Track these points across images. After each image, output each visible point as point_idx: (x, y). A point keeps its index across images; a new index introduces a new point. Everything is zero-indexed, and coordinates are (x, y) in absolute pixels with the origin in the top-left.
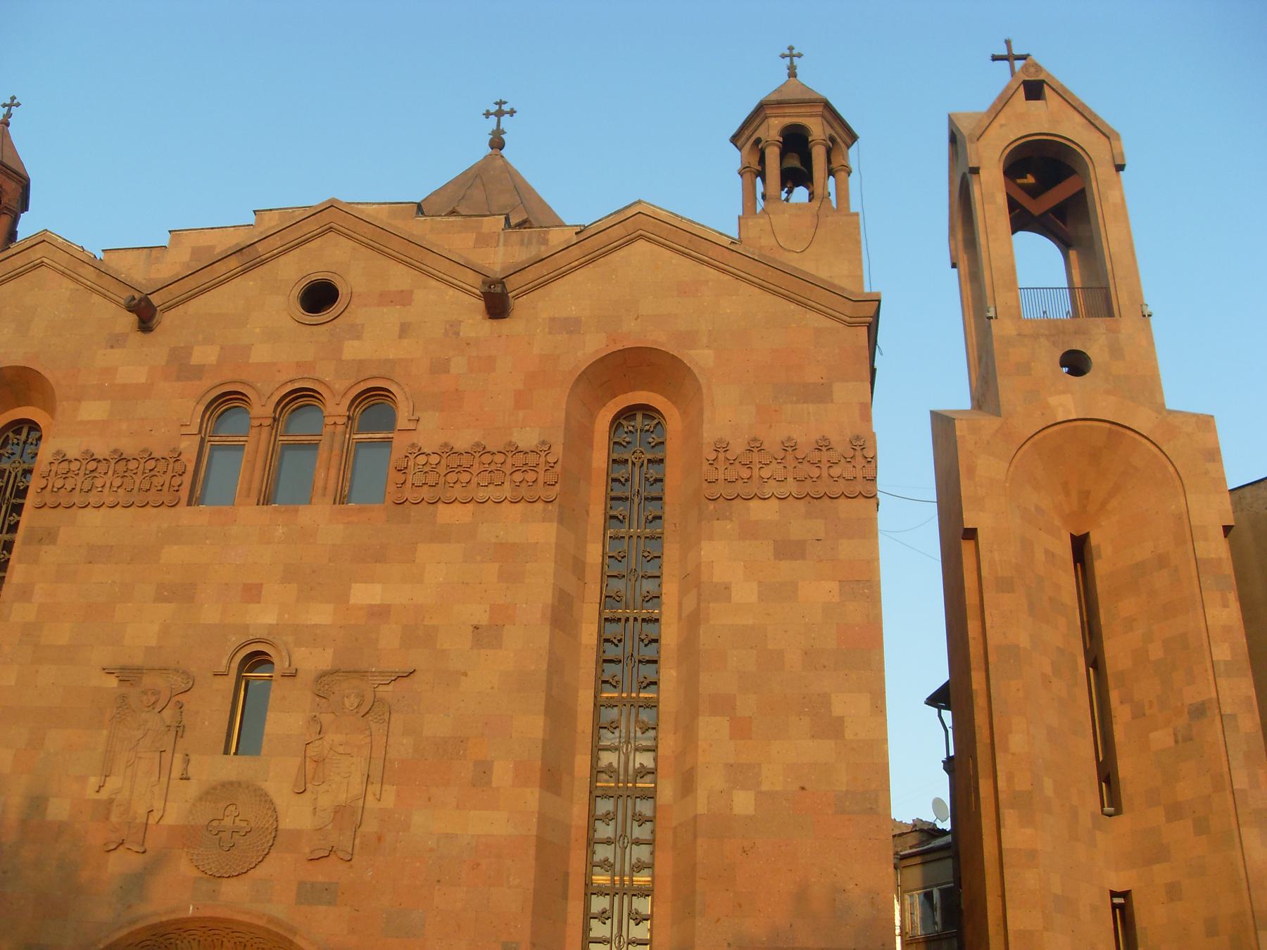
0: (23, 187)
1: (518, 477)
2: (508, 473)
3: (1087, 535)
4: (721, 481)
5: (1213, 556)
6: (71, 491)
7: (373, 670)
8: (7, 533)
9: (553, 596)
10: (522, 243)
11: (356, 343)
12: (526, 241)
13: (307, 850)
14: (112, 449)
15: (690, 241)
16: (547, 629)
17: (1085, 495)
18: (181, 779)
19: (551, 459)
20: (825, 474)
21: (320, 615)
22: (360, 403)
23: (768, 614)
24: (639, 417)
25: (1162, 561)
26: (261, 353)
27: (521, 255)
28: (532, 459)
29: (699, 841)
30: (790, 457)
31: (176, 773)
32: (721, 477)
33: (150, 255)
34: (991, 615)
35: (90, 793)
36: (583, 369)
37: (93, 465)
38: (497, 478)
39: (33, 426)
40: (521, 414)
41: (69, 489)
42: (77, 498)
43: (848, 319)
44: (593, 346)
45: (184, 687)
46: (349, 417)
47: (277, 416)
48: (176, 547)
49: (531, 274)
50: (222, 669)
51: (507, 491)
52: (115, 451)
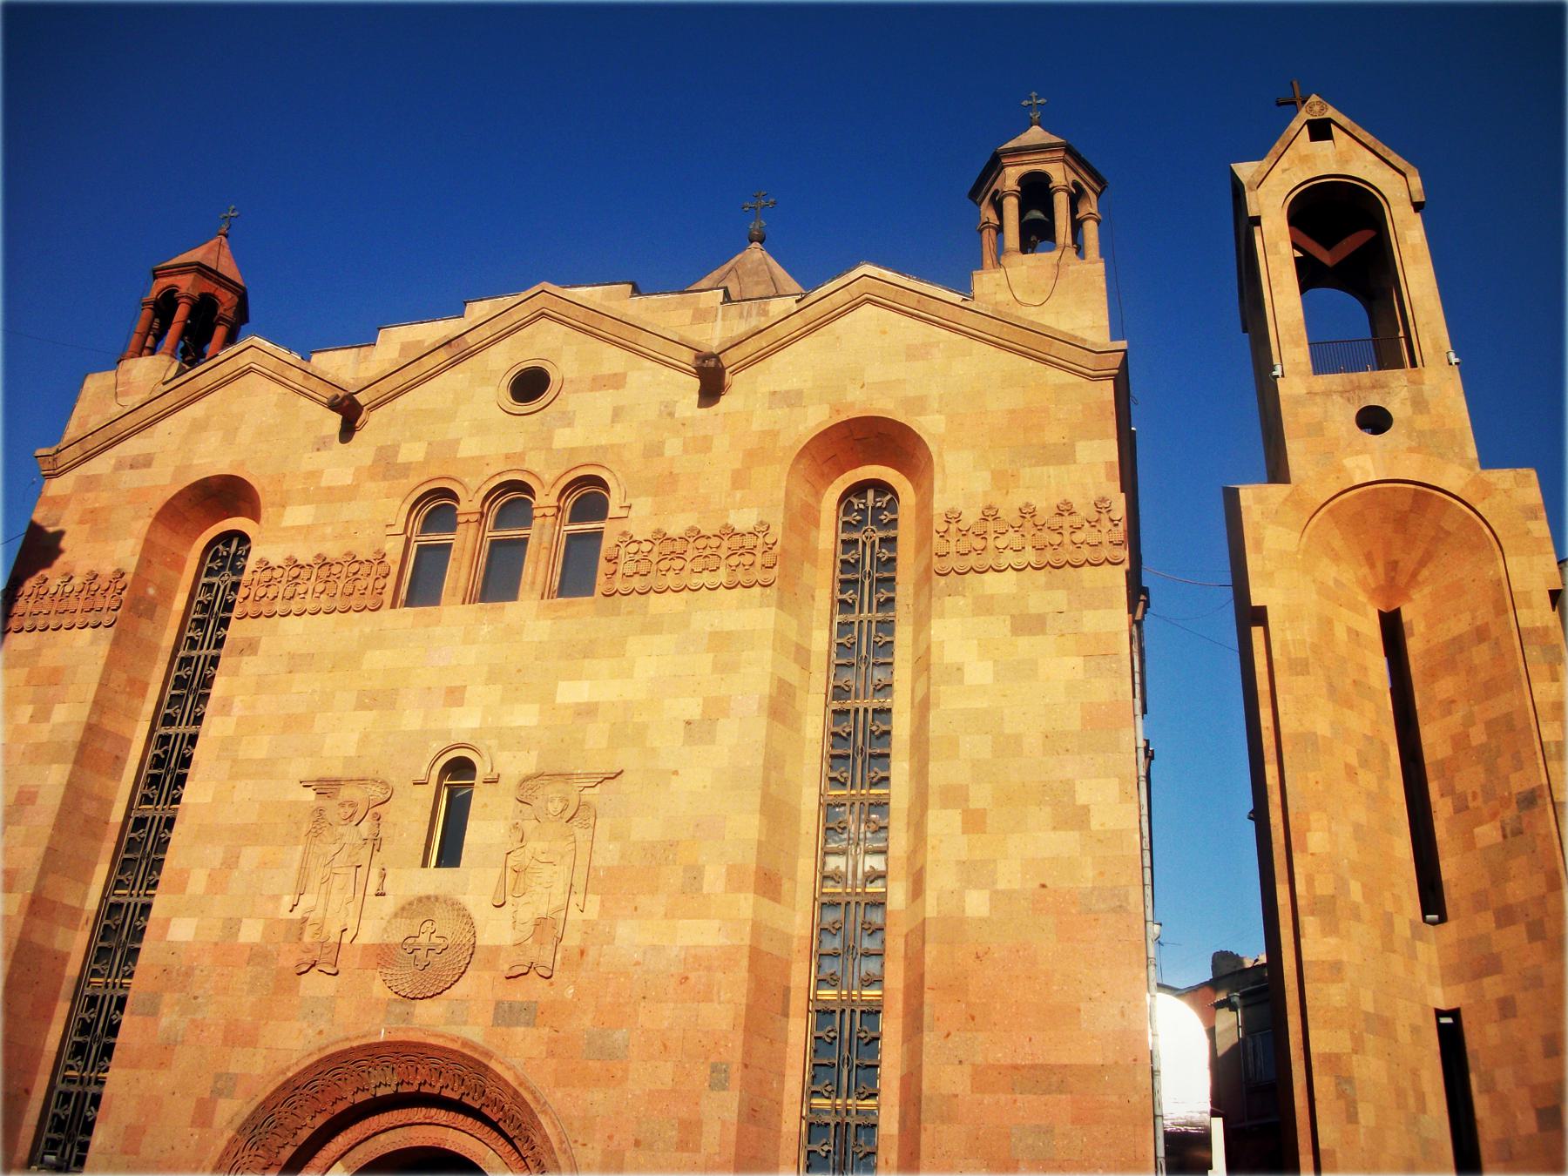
0: (239, 297)
1: (734, 560)
2: (723, 557)
3: (1398, 611)
4: (953, 555)
5: (1538, 624)
6: (273, 599)
7: (579, 772)
8: (214, 648)
9: (771, 686)
10: (741, 316)
11: (567, 431)
12: (745, 314)
13: (506, 967)
14: (315, 554)
15: (919, 301)
16: (763, 721)
17: (1392, 566)
18: (377, 895)
19: (770, 540)
20: (1067, 539)
21: (525, 716)
22: (570, 494)
23: (1005, 696)
24: (871, 494)
25: (1481, 634)
27: (740, 328)
28: (749, 542)
29: (928, 948)
30: (1028, 524)
31: (372, 889)
32: (953, 549)
33: (359, 354)
34: (1285, 701)
35: (284, 913)
36: (804, 444)
37: (296, 571)
38: (712, 563)
39: (244, 539)
40: (738, 494)
41: (271, 596)
42: (279, 606)
43: (1091, 373)
44: (816, 418)
45: (382, 798)
46: (559, 508)
47: (485, 511)
48: (378, 652)
49: (750, 347)
50: (422, 777)
51: (722, 576)
52: (318, 556)
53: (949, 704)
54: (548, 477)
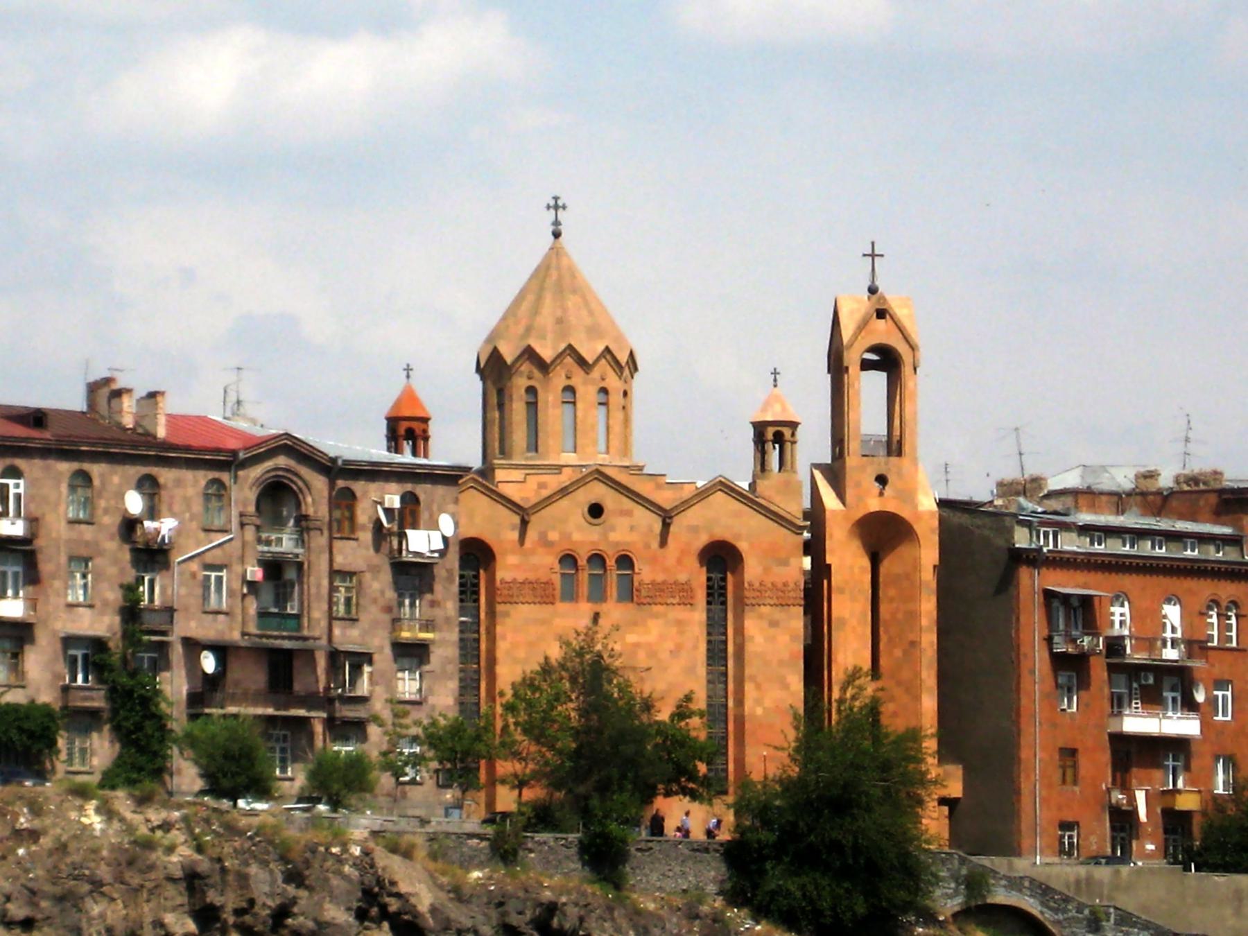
1: (681, 594)
26: (576, 537)
42: (515, 599)
53: (750, 648)
54: (610, 552)
